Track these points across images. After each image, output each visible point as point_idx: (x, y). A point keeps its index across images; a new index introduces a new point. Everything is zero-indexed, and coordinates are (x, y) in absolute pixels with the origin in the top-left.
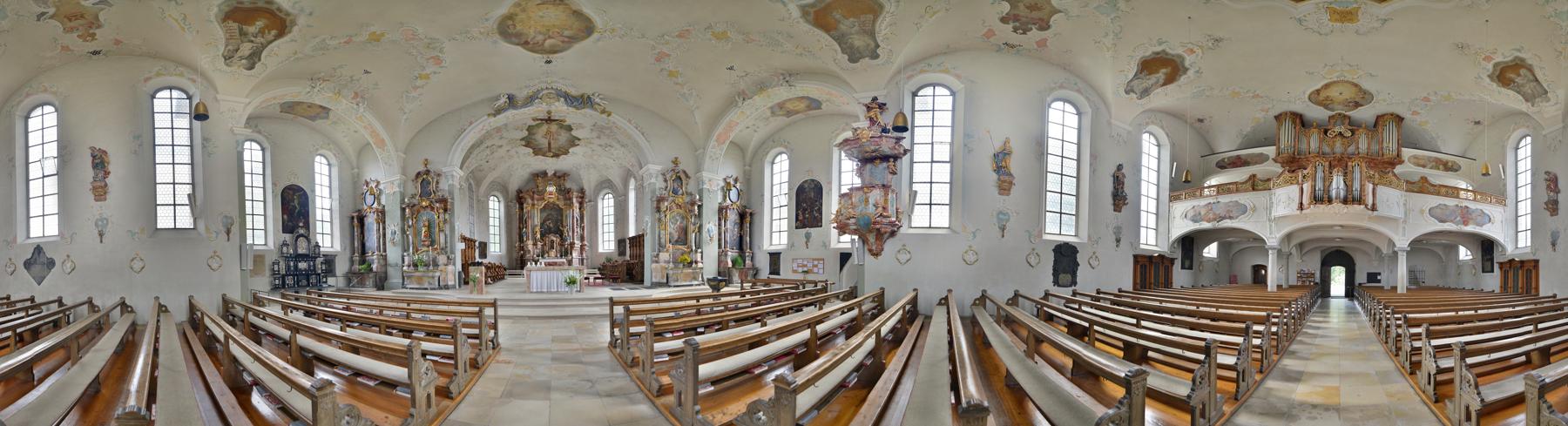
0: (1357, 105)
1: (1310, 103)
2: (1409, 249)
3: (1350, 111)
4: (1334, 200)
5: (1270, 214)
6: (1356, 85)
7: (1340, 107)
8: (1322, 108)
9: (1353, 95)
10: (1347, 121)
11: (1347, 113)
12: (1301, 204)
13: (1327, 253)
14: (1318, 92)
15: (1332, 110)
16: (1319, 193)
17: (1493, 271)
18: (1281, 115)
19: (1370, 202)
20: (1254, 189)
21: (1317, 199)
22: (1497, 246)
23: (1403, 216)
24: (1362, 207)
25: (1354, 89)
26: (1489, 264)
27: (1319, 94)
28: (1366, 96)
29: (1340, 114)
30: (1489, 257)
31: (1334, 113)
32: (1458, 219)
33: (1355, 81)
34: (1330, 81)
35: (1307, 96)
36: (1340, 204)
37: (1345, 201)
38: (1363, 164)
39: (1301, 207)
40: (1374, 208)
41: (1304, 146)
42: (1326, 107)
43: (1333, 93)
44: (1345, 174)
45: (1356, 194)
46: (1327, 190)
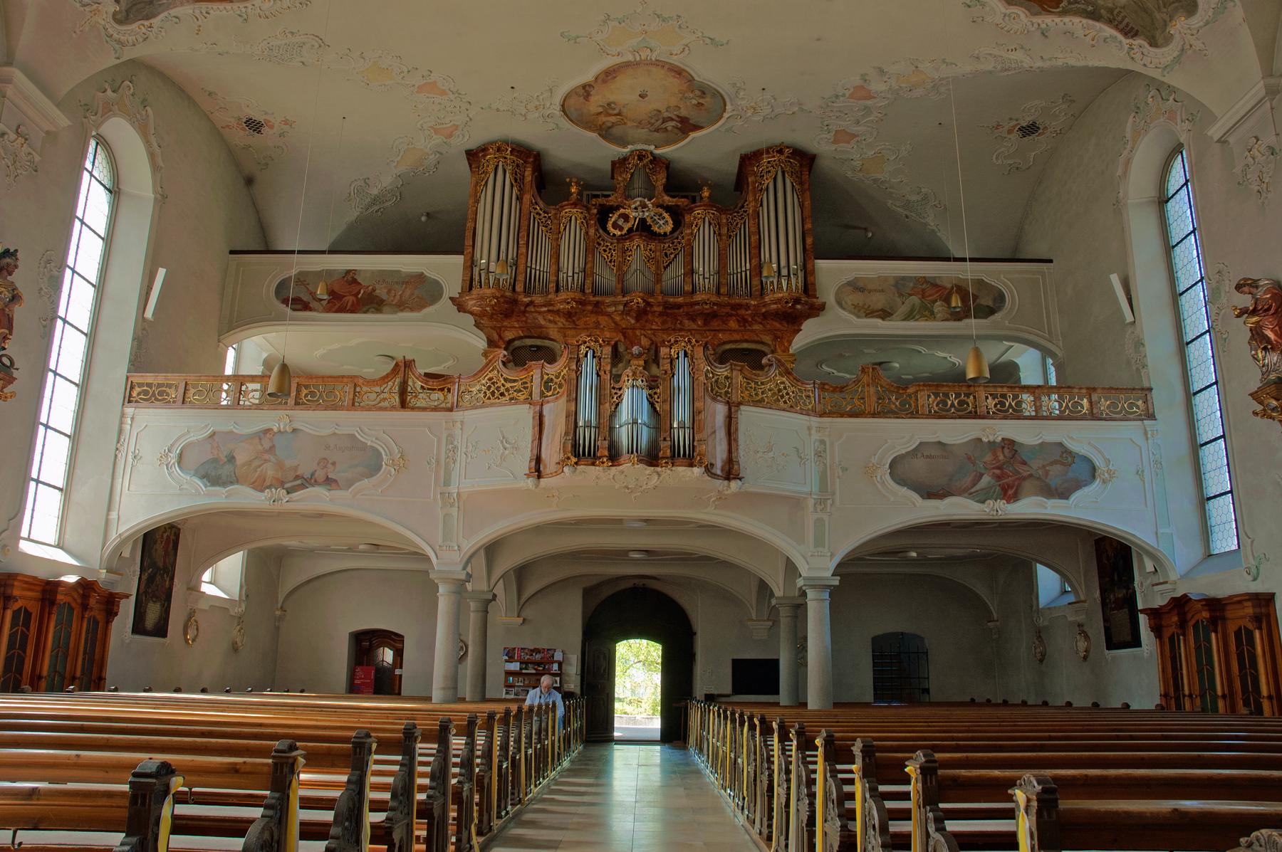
0: (686, 126)
1: (566, 124)
2: (836, 581)
3: (668, 143)
4: (625, 457)
5: (447, 483)
6: (678, 72)
7: (643, 132)
8: (595, 135)
9: (673, 102)
10: (660, 180)
11: (658, 152)
12: (538, 460)
13: (607, 592)
14: (586, 90)
15: (623, 142)
16: (586, 435)
17: (1136, 642)
18: (484, 149)
19: (719, 454)
20: (404, 404)
21: (580, 453)
22: (1140, 557)
23: (815, 489)
24: (697, 471)
25: (674, 83)
26: (1122, 616)
27: (587, 96)
28: (707, 101)
29: (641, 157)
30: (1121, 594)
31: (626, 150)
32: (986, 480)
33: (675, 60)
34: (619, 60)
35: (557, 100)
36: (641, 466)
37: (652, 458)
38: (699, 352)
39: (537, 469)
40: (730, 472)
41: (541, 265)
42: (606, 133)
43: (623, 93)
44: (652, 384)
45: (682, 437)
46: (607, 424)
